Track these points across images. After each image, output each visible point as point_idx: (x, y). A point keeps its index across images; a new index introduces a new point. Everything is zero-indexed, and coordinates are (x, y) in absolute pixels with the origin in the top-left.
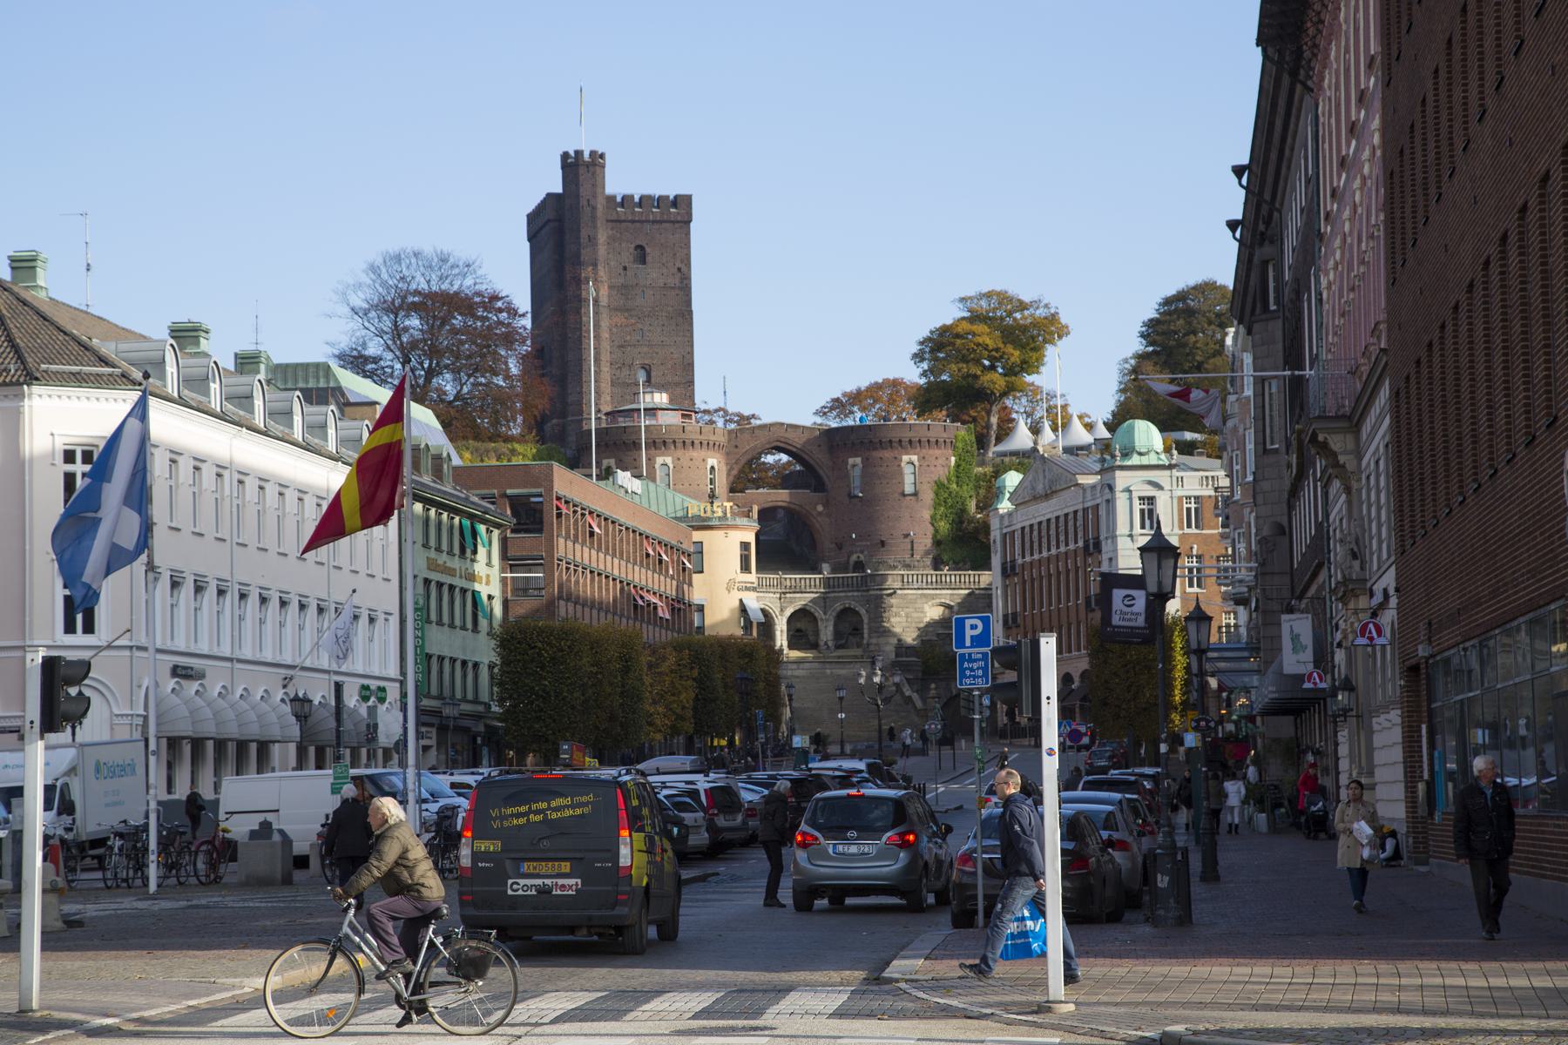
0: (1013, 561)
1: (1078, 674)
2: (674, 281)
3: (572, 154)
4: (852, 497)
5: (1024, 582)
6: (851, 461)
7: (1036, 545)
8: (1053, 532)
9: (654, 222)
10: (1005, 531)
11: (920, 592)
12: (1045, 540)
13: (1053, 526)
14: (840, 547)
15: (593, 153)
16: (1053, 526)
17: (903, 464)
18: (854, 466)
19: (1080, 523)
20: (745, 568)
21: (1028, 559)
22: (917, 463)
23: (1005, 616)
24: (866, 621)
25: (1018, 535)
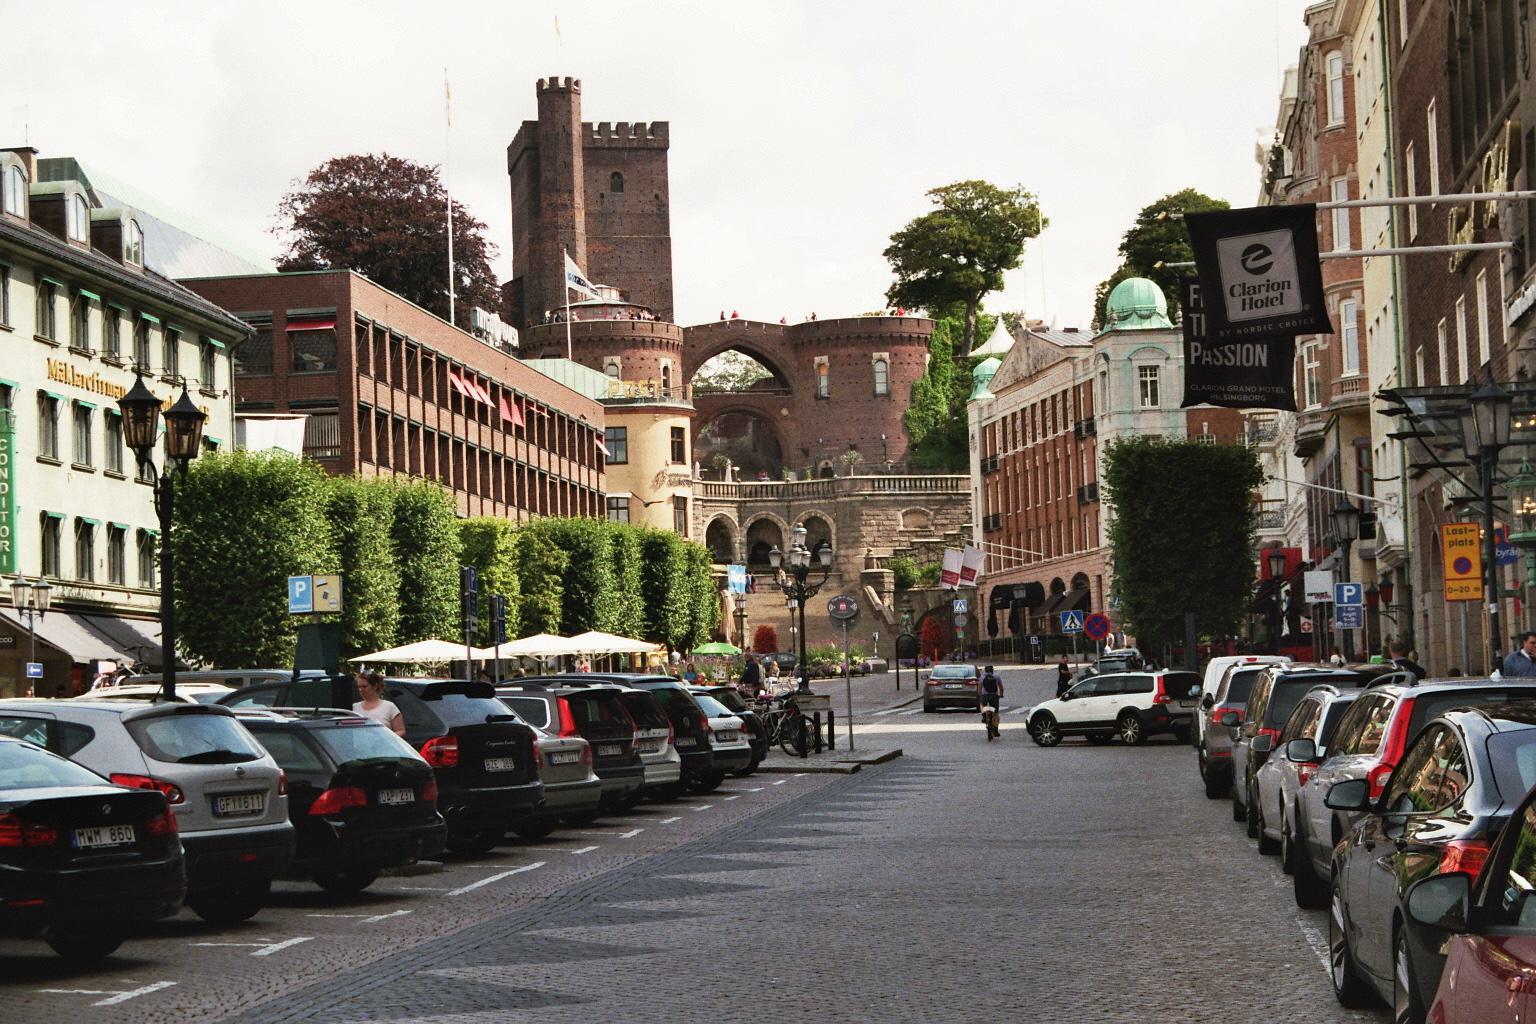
0: (994, 456)
1: (1070, 579)
2: (651, 209)
3: (547, 81)
4: (818, 397)
5: (1007, 479)
6: (817, 359)
7: (1019, 436)
8: (1038, 418)
9: (631, 149)
10: (984, 424)
11: (892, 498)
12: (1029, 429)
13: (1039, 412)
14: (806, 452)
15: (568, 80)
16: (1039, 412)
17: (873, 362)
18: (821, 365)
19: (1070, 403)
20: (678, 456)
21: (1011, 452)
22: (888, 361)
23: (986, 520)
24: (834, 531)
25: (999, 427)
